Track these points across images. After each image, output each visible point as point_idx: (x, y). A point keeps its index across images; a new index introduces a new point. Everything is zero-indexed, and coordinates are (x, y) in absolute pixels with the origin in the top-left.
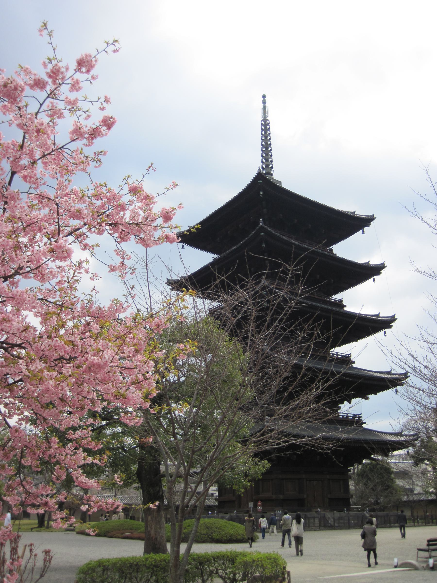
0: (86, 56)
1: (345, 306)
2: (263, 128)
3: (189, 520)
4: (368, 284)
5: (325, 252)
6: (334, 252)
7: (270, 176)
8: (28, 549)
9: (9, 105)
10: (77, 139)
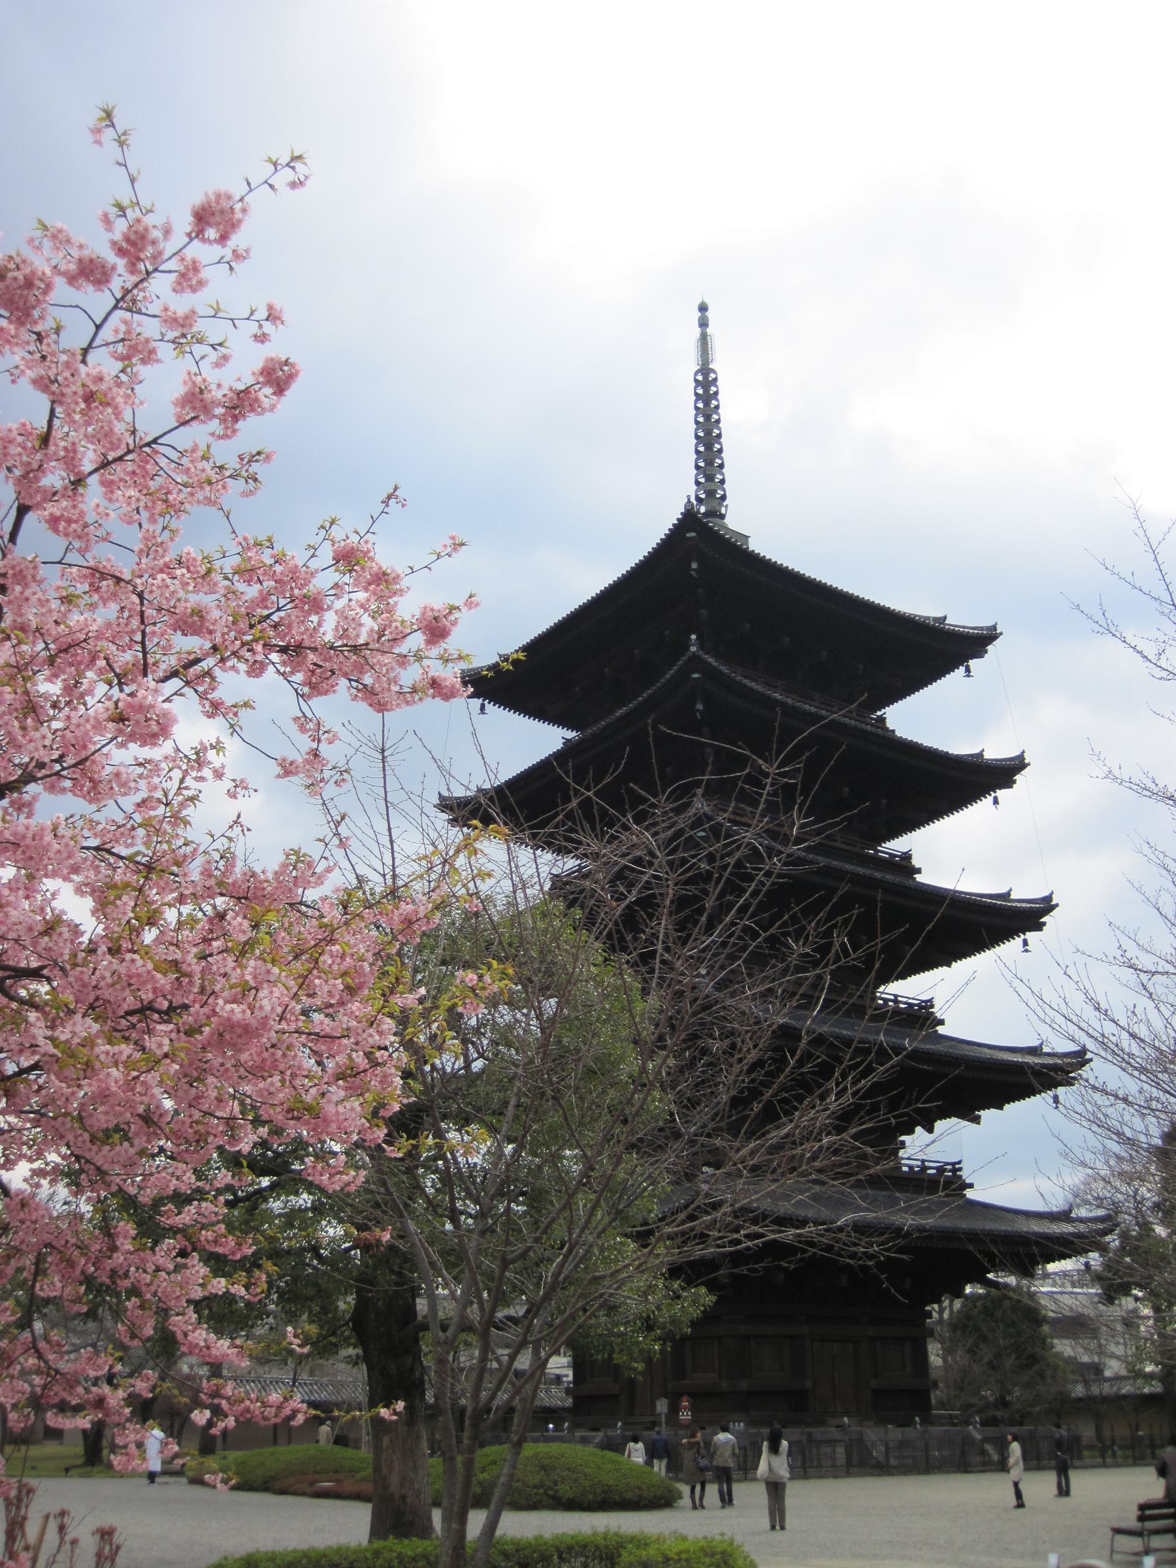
0: (218, 196)
1: (919, 871)
2: (700, 391)
3: (495, 1448)
4: (979, 812)
5: (864, 726)
6: (890, 725)
7: (717, 520)
8: (53, 1525)
9: (12, 329)
10: (193, 419)
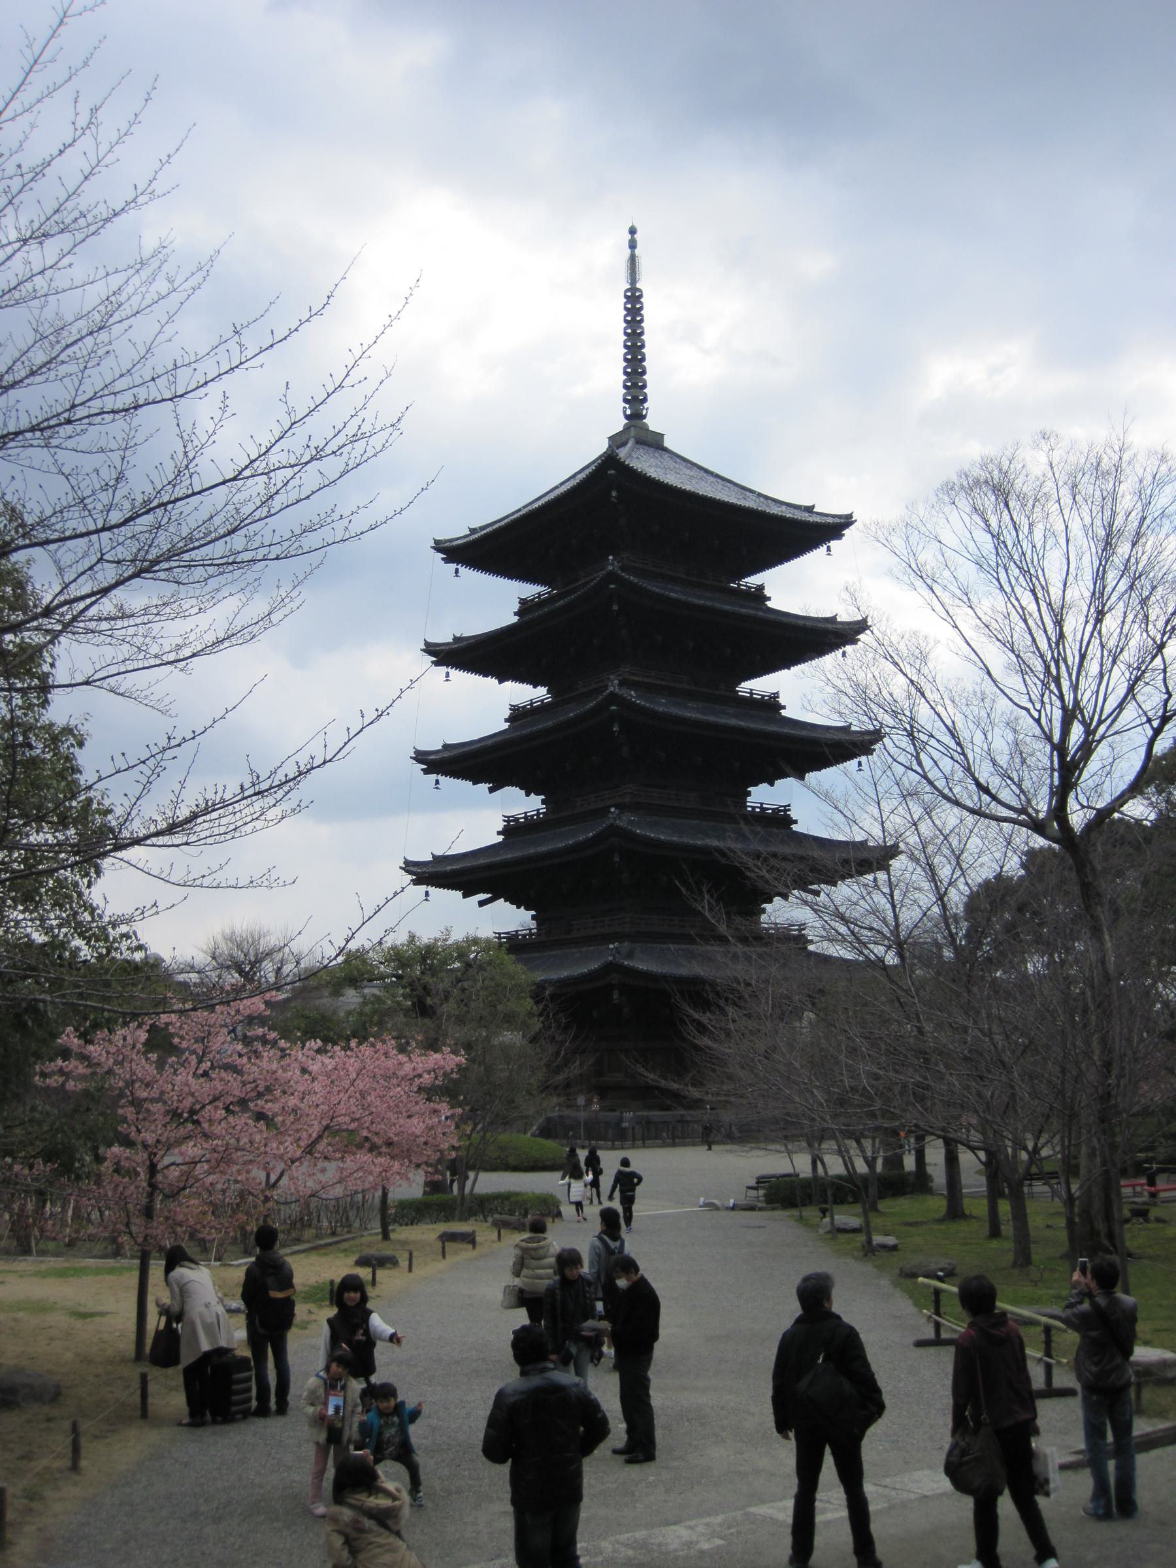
1: (784, 707)
4: (829, 661)
6: (767, 592)
